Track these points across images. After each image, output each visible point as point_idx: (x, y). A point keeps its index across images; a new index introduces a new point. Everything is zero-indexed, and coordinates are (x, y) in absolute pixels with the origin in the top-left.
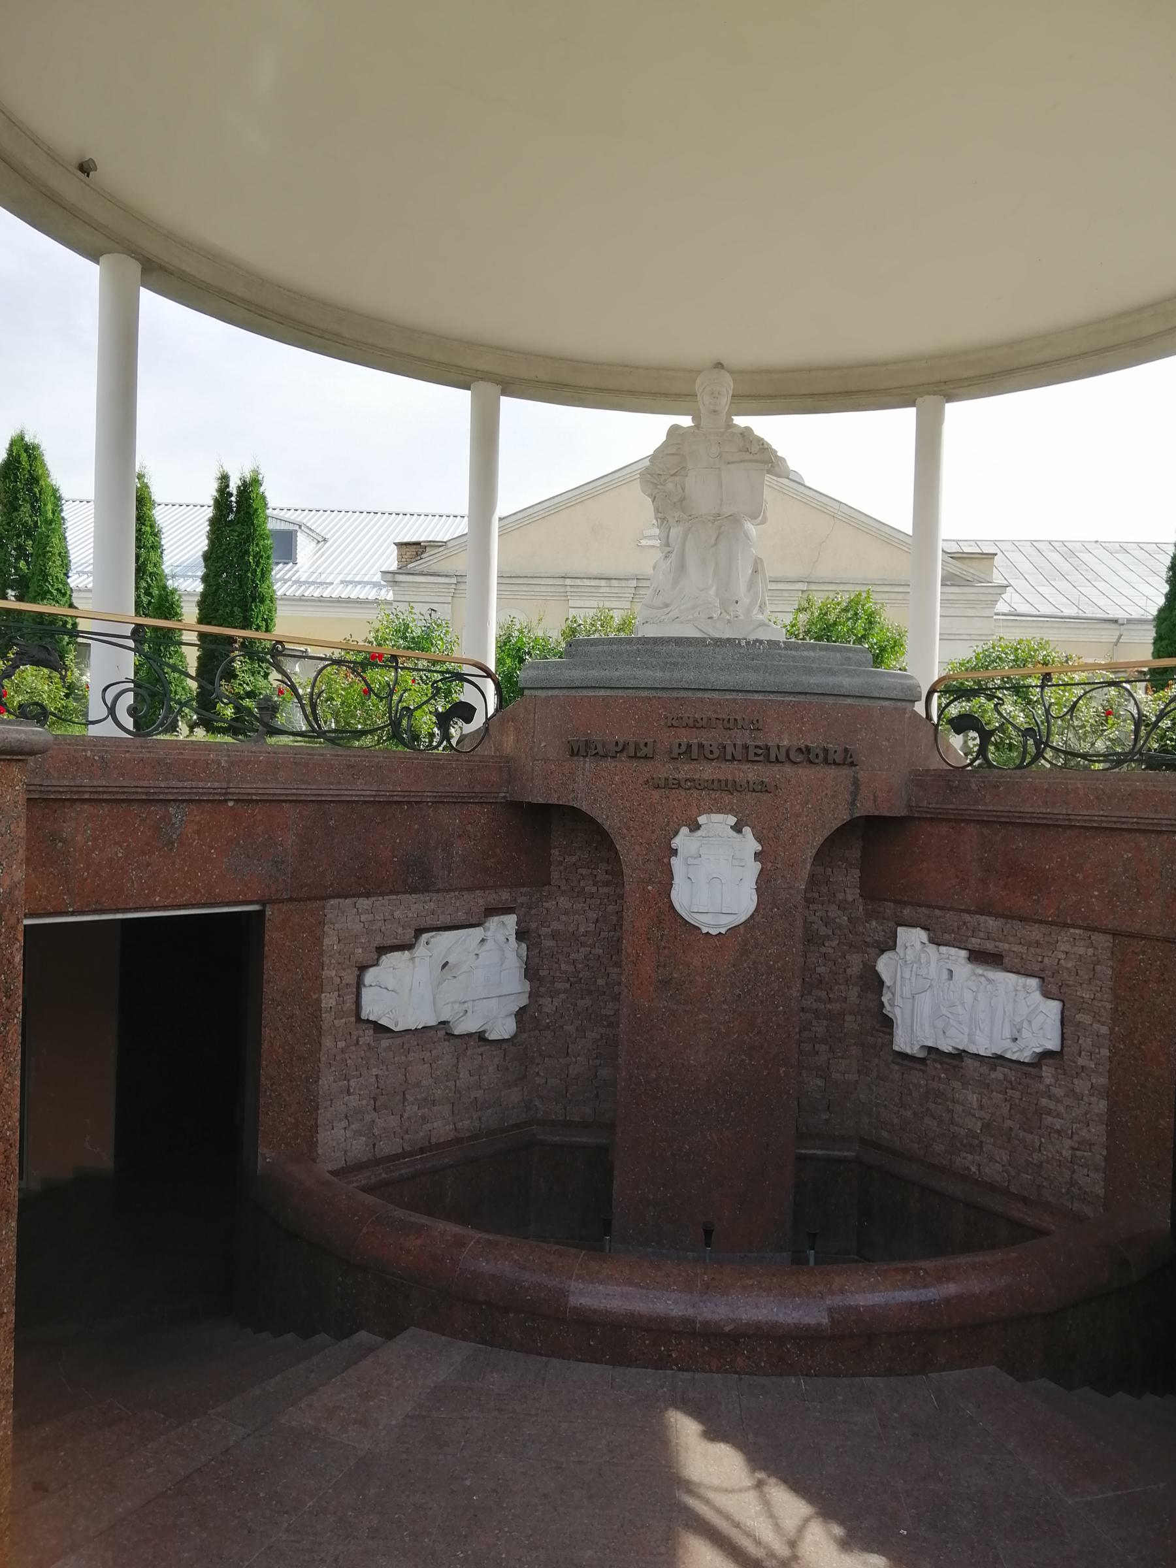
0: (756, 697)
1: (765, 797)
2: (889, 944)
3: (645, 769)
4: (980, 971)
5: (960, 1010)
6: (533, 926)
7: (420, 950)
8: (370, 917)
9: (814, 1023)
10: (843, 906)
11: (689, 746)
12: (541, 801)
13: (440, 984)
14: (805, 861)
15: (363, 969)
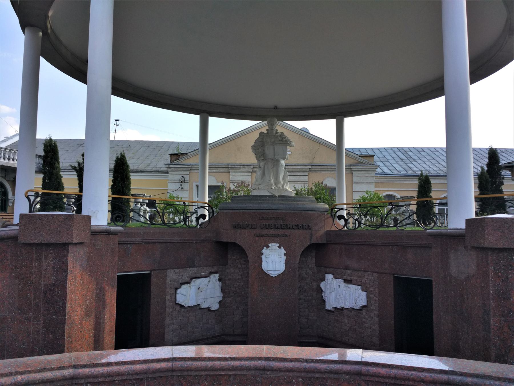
0: (284, 211)
1: (287, 238)
2: (323, 279)
3: (254, 231)
4: (346, 285)
5: (342, 296)
6: (223, 277)
7: (192, 284)
11: (266, 225)
12: (225, 241)
13: (198, 293)
15: (177, 289)
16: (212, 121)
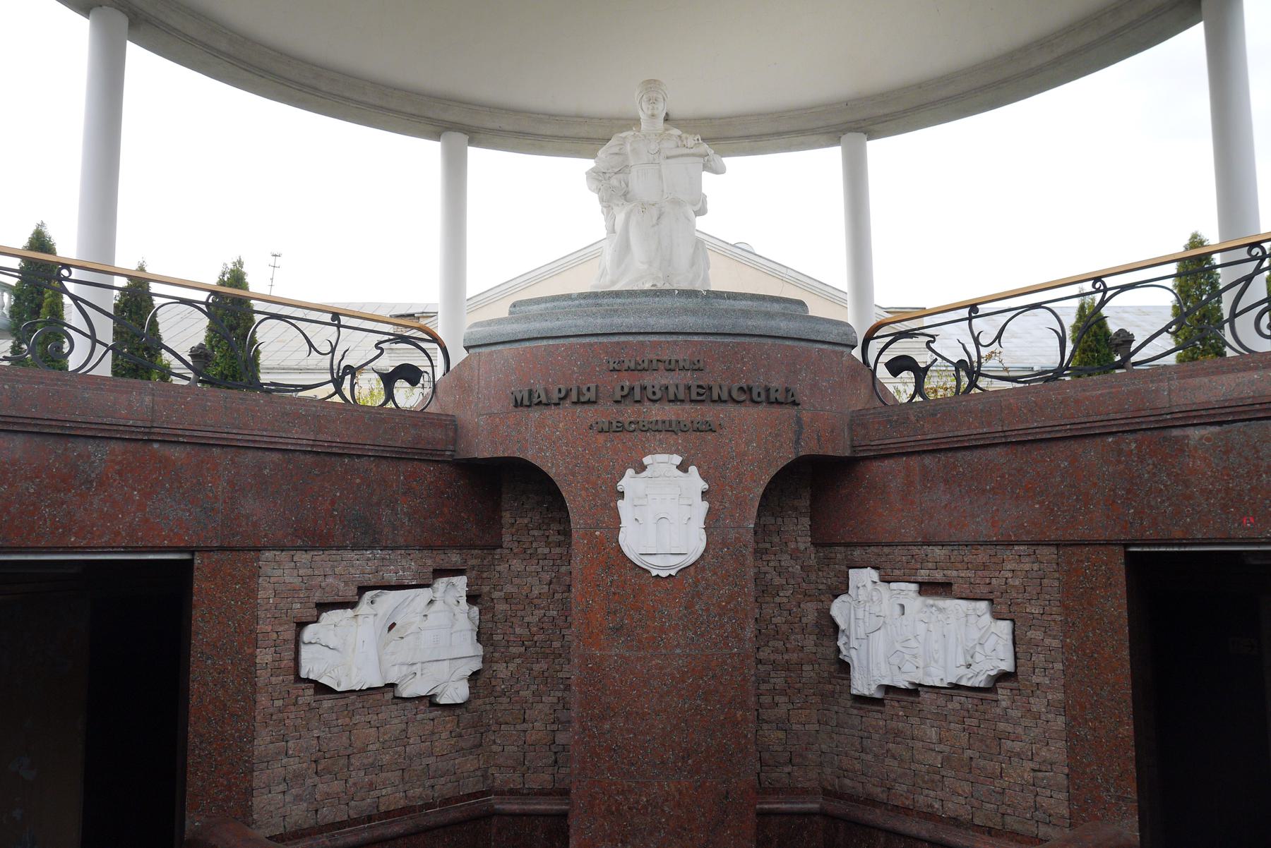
0: (696, 338)
1: (709, 436)
2: (841, 588)
3: (589, 414)
4: (930, 601)
6: (486, 589)
7: (364, 607)
8: (309, 572)
9: (772, 674)
10: (795, 555)
12: (487, 455)
13: (387, 644)
15: (301, 625)
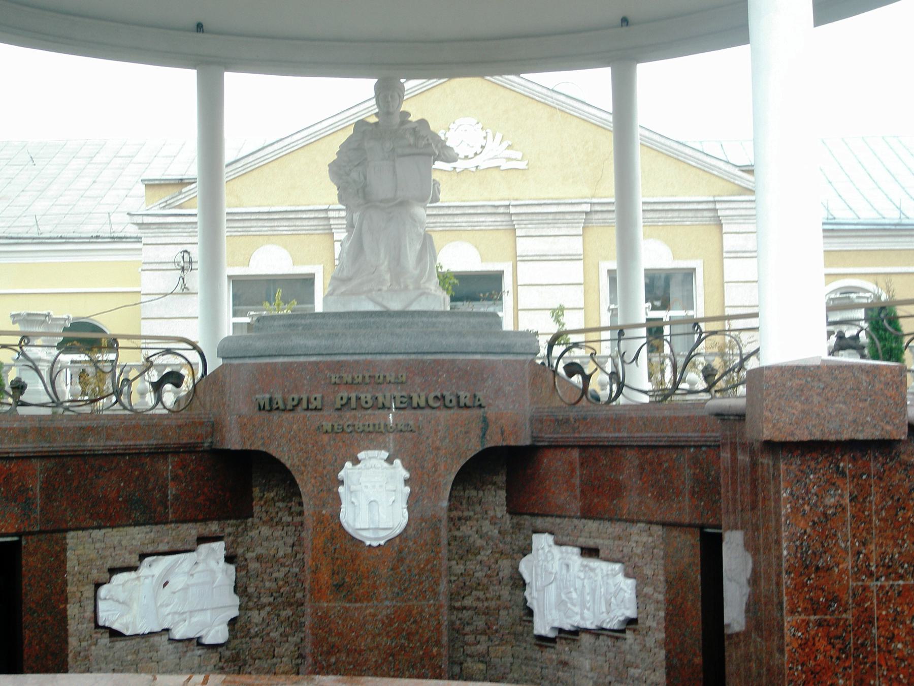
2: (526, 550)
5: (574, 595)
6: (240, 551)
7: (144, 570)
8: (103, 545)
9: (475, 617)
10: (493, 522)
14: (445, 484)
15: (98, 585)
16: (237, 85)
